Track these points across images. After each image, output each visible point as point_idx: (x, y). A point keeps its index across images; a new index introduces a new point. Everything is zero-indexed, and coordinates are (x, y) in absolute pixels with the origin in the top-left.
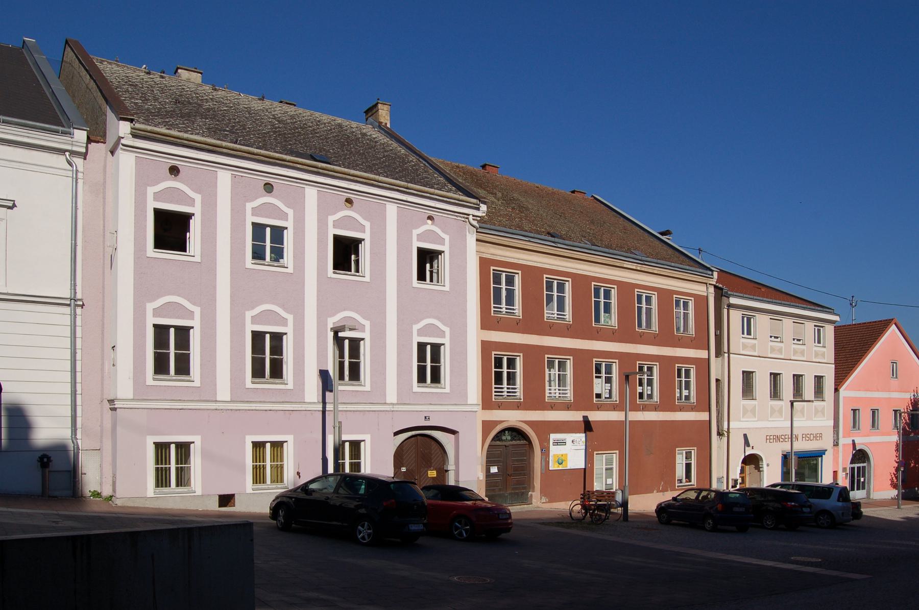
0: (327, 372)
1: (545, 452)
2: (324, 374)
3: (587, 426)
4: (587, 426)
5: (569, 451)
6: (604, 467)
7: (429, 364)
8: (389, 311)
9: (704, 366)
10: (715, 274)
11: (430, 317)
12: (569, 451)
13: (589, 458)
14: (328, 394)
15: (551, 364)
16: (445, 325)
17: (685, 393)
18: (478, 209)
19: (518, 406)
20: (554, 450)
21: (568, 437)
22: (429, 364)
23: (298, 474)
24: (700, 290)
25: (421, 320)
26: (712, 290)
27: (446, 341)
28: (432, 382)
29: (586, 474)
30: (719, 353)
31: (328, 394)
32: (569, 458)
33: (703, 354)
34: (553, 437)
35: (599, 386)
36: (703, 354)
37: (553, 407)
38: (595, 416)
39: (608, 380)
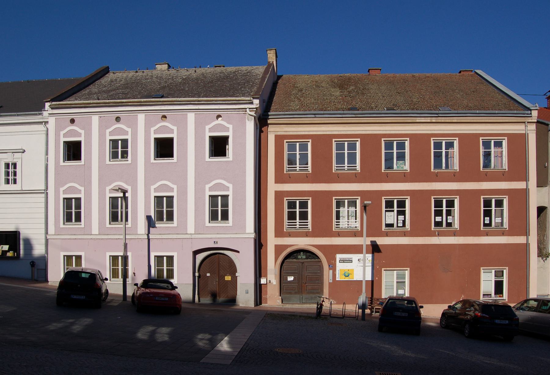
0: (150, 216)
1: (333, 267)
2: (149, 218)
3: (375, 248)
4: (375, 248)
5: (356, 268)
6: (395, 281)
7: (219, 209)
8: (192, 177)
9: (520, 198)
10: (535, 113)
11: (217, 179)
12: (356, 268)
13: (376, 272)
14: (151, 229)
15: (339, 204)
16: (229, 182)
17: (499, 220)
18: (252, 103)
19: (307, 235)
20: (340, 266)
21: (355, 257)
22: (219, 209)
23: (134, 273)
24: (517, 129)
25: (212, 181)
26: (533, 127)
27: (230, 193)
28: (222, 219)
29: (374, 285)
30: (542, 183)
31: (151, 229)
32: (355, 272)
33: (520, 185)
34: (339, 256)
35: (390, 217)
36: (520, 185)
37: (339, 234)
38: (381, 241)
39: (402, 213)
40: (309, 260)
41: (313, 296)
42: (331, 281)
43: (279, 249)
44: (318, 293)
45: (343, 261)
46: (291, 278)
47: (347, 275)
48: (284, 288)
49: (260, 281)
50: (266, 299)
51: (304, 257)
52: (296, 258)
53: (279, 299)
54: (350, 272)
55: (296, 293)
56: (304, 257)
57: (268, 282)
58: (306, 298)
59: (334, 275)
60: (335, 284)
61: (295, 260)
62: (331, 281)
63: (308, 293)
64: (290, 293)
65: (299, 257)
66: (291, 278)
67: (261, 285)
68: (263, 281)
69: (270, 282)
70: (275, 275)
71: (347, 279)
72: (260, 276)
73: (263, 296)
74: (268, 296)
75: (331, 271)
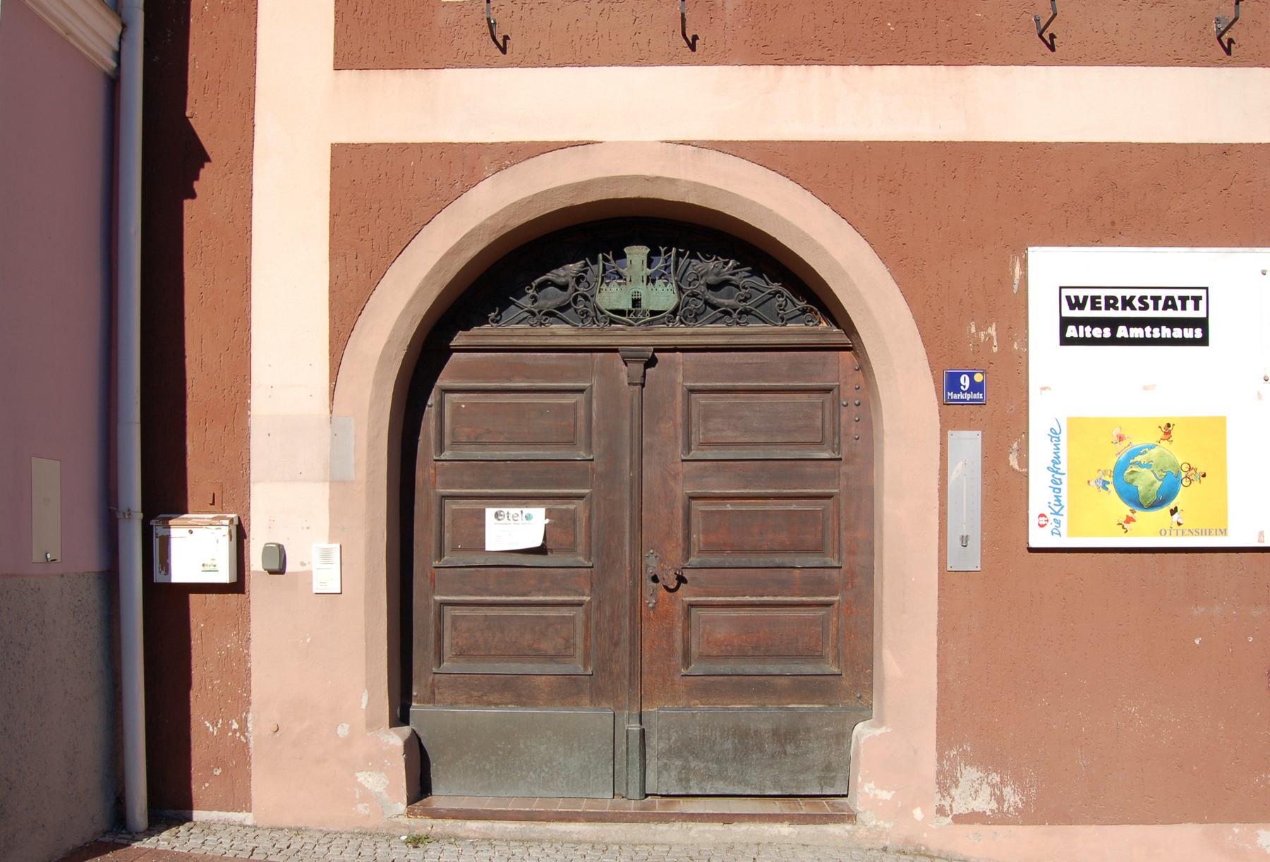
1: (981, 390)
20: (1068, 388)
40: (712, 331)
41: (761, 715)
42: (969, 559)
43: (375, 193)
44: (818, 688)
45: (1099, 323)
46: (514, 529)
47: (1146, 481)
48: (455, 619)
49: (155, 552)
50: (238, 758)
51: (663, 297)
52: (576, 306)
53: (374, 763)
54: (1178, 453)
55: (569, 690)
56: (663, 297)
57: (255, 562)
58: (686, 749)
59: (1005, 490)
60: (1010, 577)
61: (560, 332)
62: (969, 559)
63: (707, 688)
64: (513, 690)
65: (613, 296)
66: (514, 529)
67: (169, 605)
68: (196, 552)
69: (278, 564)
70: (337, 484)
71: (1151, 530)
72: (167, 496)
73: (205, 726)
74: (258, 724)
75: (967, 446)
